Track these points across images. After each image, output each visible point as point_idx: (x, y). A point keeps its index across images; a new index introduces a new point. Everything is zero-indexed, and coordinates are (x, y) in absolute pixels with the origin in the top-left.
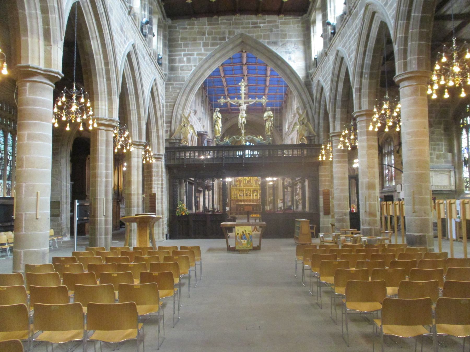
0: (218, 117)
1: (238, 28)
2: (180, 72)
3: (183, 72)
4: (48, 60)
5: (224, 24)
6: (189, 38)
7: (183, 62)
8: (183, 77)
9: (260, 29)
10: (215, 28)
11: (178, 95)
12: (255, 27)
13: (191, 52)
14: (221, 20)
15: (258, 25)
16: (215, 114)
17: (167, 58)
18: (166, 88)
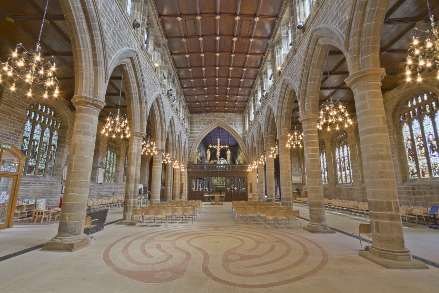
1: (217, 118)
4: (162, 147)
5: (212, 116)
7: (195, 131)
16: (207, 151)
17: (189, 129)
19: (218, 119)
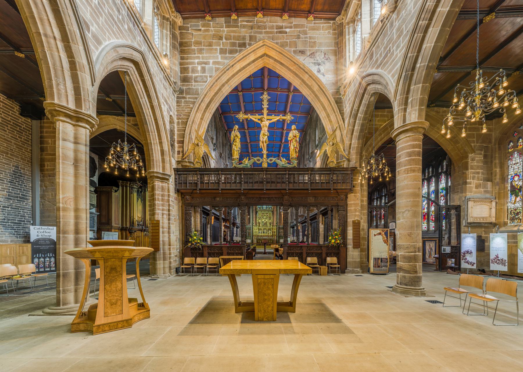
0: (236, 136)
1: (261, 33)
2: (193, 83)
3: (196, 83)
5: (244, 26)
6: (203, 42)
8: (197, 89)
9: (285, 35)
10: (234, 32)
11: (191, 111)
12: (280, 32)
13: (206, 61)
14: (242, 21)
15: (284, 30)
16: (233, 132)
18: (177, 102)
19: (261, 36)
